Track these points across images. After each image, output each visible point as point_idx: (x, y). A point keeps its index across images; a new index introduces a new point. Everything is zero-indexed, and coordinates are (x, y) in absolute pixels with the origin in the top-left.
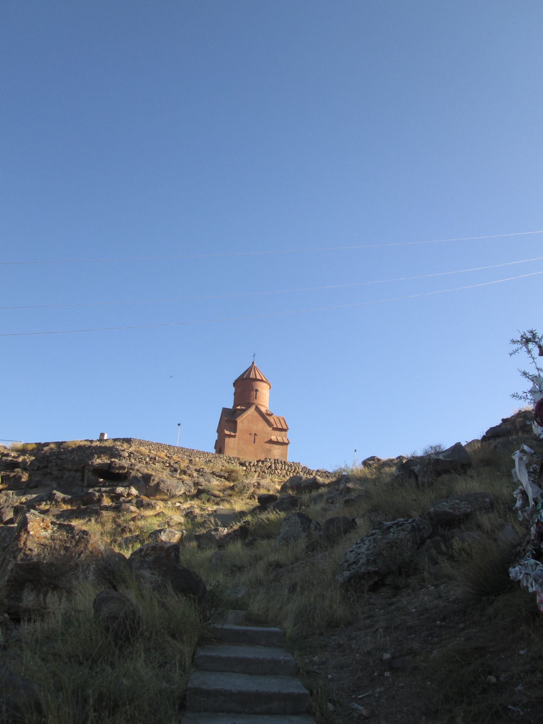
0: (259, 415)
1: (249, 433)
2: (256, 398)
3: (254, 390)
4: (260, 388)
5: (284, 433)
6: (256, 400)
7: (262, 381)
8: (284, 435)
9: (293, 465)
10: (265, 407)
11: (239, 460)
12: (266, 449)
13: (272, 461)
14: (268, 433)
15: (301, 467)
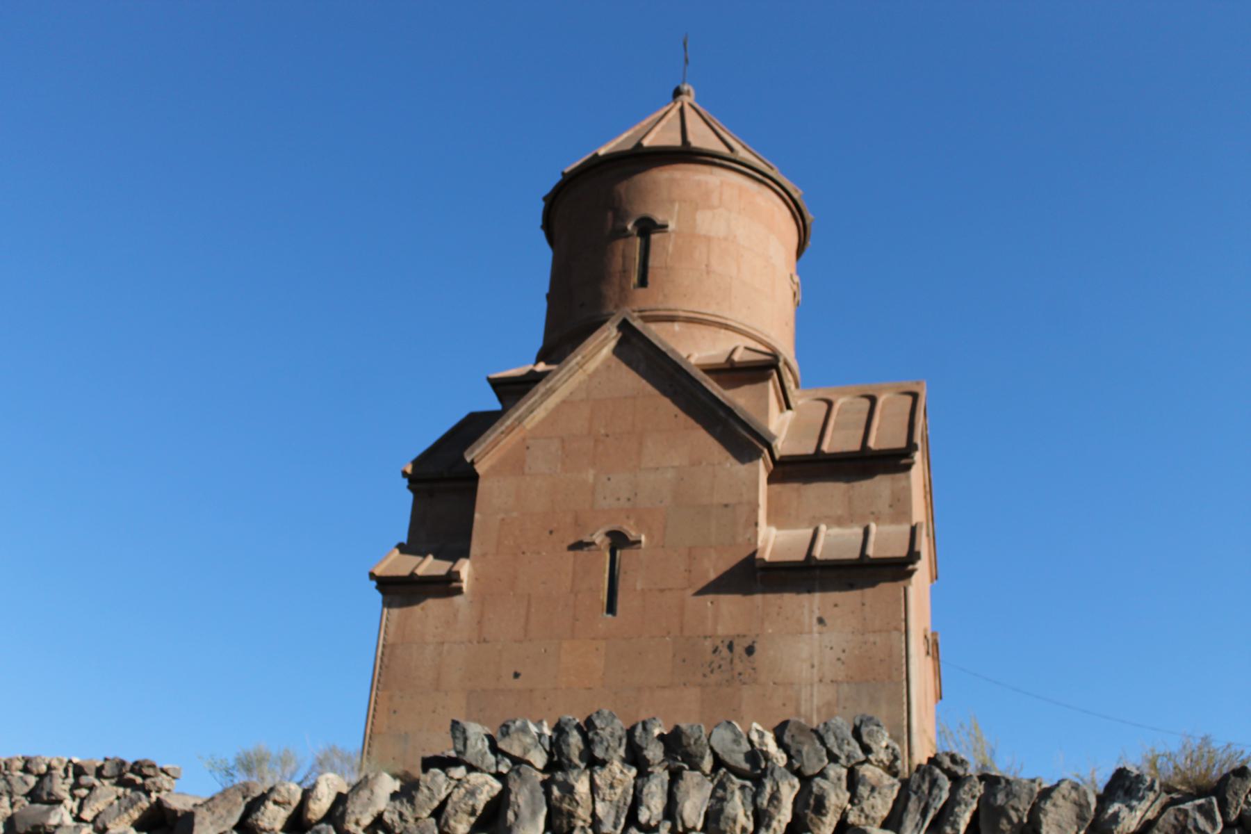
0: (649, 388)
1: (572, 541)
2: (643, 282)
3: (630, 226)
4: (677, 206)
5: (881, 485)
6: (641, 291)
7: (685, 155)
8: (883, 505)
9: (780, 758)
10: (727, 327)
11: (148, 793)
12: (708, 644)
13: (516, 751)
14: (726, 506)
15: (891, 770)
